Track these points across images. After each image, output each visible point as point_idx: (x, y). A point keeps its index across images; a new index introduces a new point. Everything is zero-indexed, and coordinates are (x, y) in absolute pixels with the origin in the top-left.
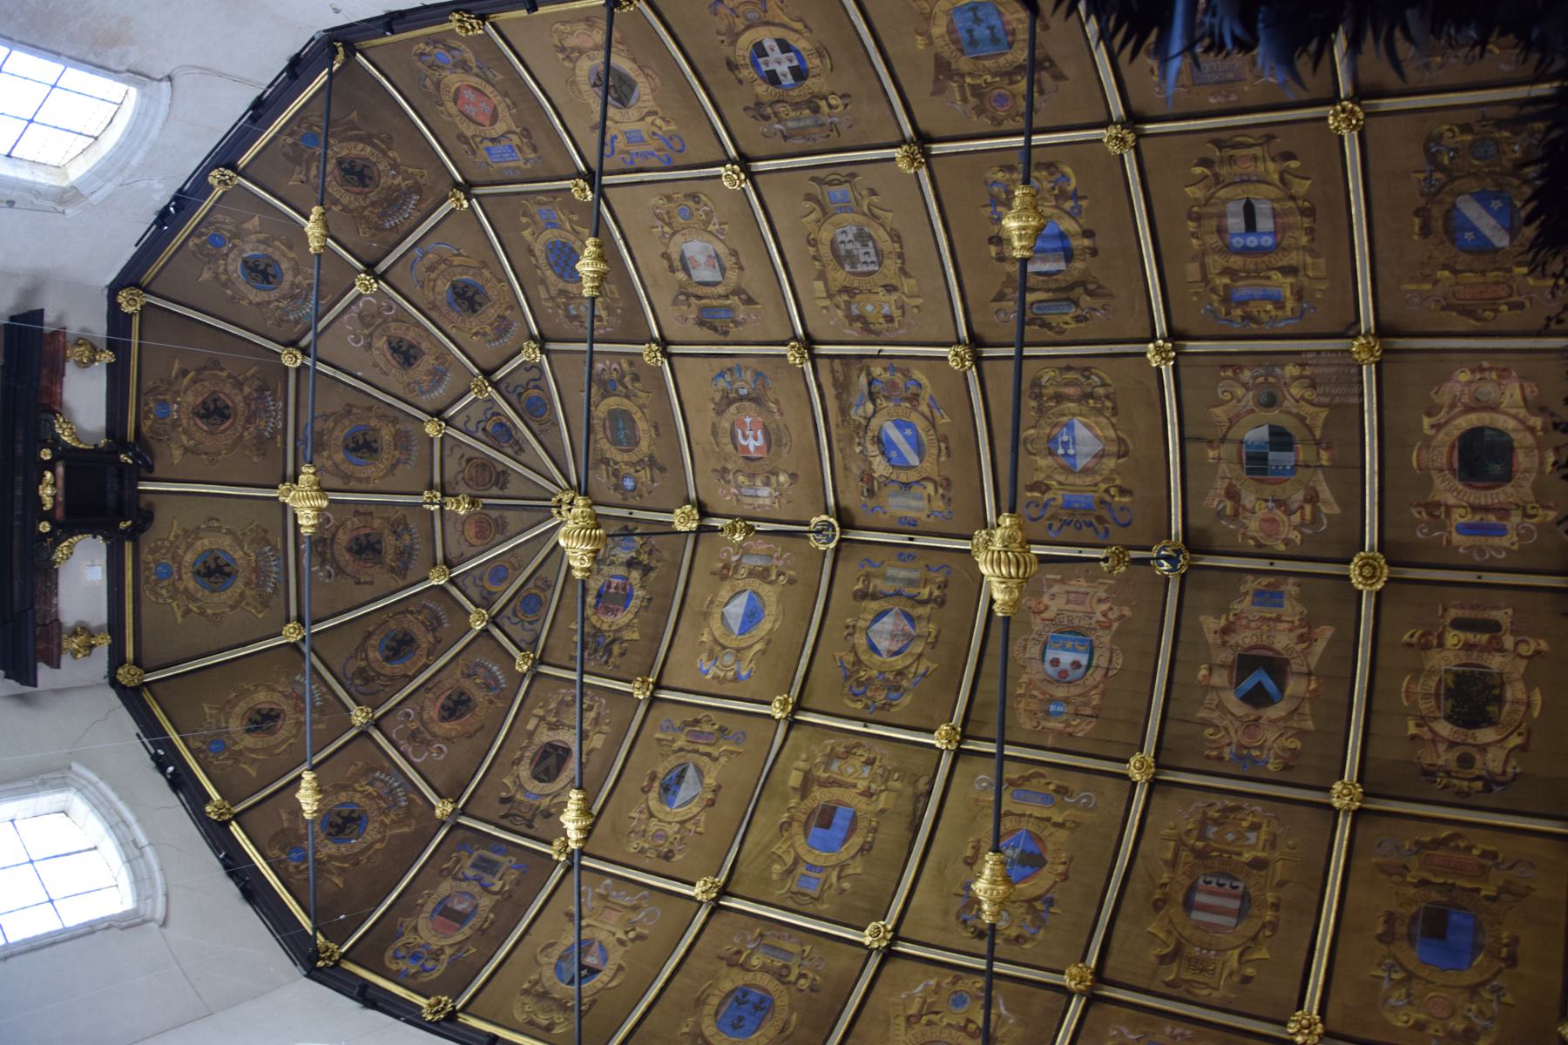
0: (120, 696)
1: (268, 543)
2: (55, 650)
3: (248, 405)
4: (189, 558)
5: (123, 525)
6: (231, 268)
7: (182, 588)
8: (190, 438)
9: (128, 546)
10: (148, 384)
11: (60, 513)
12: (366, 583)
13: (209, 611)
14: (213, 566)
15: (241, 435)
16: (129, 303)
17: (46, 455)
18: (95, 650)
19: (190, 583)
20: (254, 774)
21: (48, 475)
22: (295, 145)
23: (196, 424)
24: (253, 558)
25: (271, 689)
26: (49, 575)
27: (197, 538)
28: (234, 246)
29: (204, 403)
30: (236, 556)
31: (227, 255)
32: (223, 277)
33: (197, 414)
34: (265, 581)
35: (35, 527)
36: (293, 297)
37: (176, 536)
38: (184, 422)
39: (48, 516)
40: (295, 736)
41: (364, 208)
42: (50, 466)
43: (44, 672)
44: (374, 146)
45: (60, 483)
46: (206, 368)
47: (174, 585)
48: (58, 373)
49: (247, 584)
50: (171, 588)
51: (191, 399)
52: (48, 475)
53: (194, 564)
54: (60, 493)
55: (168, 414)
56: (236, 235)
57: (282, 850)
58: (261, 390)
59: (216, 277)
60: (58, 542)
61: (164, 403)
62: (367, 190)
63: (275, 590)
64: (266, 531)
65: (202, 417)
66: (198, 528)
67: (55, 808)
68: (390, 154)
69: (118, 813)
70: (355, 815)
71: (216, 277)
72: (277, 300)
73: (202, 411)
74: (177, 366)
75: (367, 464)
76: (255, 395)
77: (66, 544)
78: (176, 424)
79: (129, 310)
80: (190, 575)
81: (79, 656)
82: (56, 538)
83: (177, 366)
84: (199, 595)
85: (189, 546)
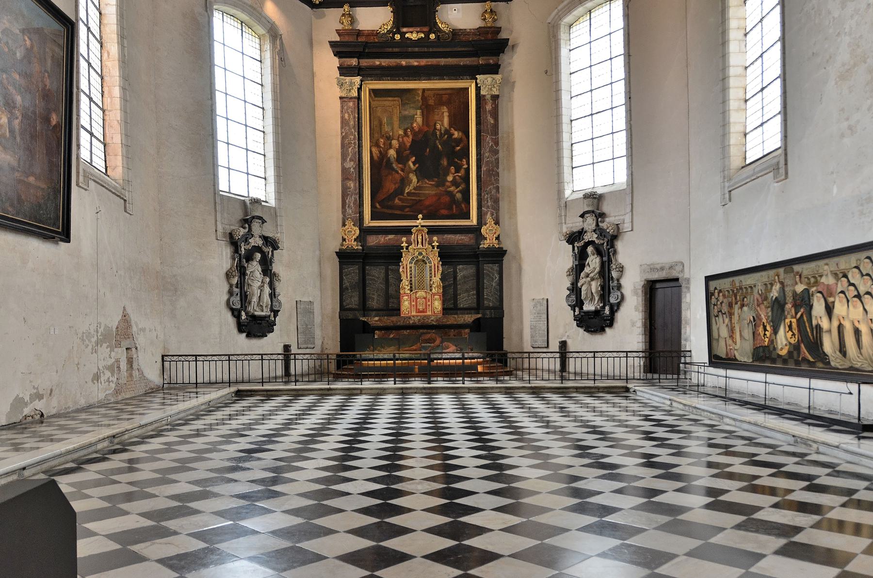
2: (493, 29)
11: (426, 29)
17: (397, 37)
18: (494, 9)
21: (407, 35)
26: (456, 33)
35: (433, 42)
42: (403, 34)
43: (503, 35)
45: (411, 29)
48: (359, 33)
52: (407, 35)
54: (415, 30)
60: (440, 30)
77: (440, 25)
81: (496, 17)
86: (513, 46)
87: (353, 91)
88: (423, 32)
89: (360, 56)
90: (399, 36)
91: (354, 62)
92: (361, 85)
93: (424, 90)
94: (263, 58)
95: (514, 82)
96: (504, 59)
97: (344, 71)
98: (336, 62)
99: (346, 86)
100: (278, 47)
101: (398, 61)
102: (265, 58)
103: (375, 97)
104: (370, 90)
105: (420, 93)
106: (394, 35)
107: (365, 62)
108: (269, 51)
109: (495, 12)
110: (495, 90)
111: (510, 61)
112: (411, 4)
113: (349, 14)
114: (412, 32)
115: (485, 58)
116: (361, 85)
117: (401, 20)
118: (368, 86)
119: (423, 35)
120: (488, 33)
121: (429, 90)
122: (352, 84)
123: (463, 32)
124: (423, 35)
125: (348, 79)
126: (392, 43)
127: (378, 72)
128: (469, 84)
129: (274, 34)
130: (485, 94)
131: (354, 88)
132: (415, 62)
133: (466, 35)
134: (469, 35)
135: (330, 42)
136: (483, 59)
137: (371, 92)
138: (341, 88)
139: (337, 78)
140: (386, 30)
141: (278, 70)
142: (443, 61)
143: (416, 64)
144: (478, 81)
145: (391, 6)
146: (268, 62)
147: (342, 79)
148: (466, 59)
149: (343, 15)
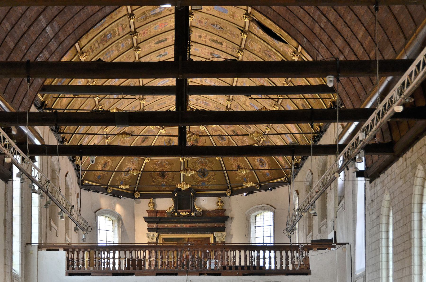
0: (233, 195)
3: (160, 167)
4: (200, 179)
5: (192, 195)
6: (127, 178)
7: (207, 180)
8: (170, 179)
9: (197, 192)
10: (157, 189)
11: (189, 211)
12: (205, 141)
13: (213, 174)
14: (202, 173)
15: (168, 168)
17: (176, 214)
19: (206, 179)
20: (251, 175)
21: (180, 213)
22: (100, 179)
23: (166, 178)
24: (200, 165)
25: (232, 164)
27: (195, 177)
28: (123, 179)
29: (161, 177)
30: (199, 169)
31: (125, 180)
32: (130, 178)
33: (164, 178)
34: (205, 162)
36: (133, 164)
37: (194, 182)
38: (166, 181)
39: (190, 213)
40: (243, 164)
41: (112, 161)
42: (178, 213)
44: (98, 165)
45: (182, 211)
46: (152, 176)
47: (206, 182)
48: (157, 212)
49: (206, 166)
50: (208, 183)
51: (160, 179)
52: (180, 213)
53: (201, 178)
56: (120, 180)
57: (267, 177)
58: (156, 165)
59: (130, 179)
60: (196, 211)
61: (162, 185)
62: (108, 162)
63: (207, 160)
64: (193, 162)
65: (164, 177)
66: (192, 177)
67: (254, 218)
68: (100, 162)
69: (255, 208)
70: (260, 160)
71: (130, 179)
72: (134, 166)
73: (163, 177)
74: (152, 183)
75: (174, 141)
76: (158, 166)
77: (196, 208)
78: (166, 182)
79: (139, 195)
80: (204, 178)
81: (223, 205)
82: (195, 211)
83: (152, 183)
84: (209, 176)
85: (197, 179)
86: (232, 218)
87: (154, 239)
89: (157, 223)
90: (177, 214)
91: (155, 225)
92: (158, 237)
93: (189, 238)
94: (114, 230)
95: (232, 235)
96: (227, 224)
97: (150, 230)
98: (146, 225)
99: (151, 237)
100: (121, 224)
101: (176, 225)
102: (115, 230)
103: (165, 241)
104: (162, 238)
105: (187, 240)
106: (174, 213)
107: (160, 225)
108: (117, 227)
109: (223, 202)
110: (223, 239)
111: (230, 224)
112: (183, 197)
113: (153, 202)
114: (183, 212)
115: (218, 224)
116: (158, 237)
118: (162, 236)
119: (188, 214)
120: (220, 212)
121: (191, 238)
122: (153, 236)
123: (207, 211)
124: (188, 214)
125: (152, 234)
127: (166, 230)
128: (210, 236)
129: (119, 219)
130: (218, 241)
131: (155, 238)
132: (184, 225)
133: (209, 212)
134: (211, 212)
135: (144, 217)
136: (217, 225)
137: (163, 239)
138: (148, 238)
139: (147, 234)
140: (170, 211)
141: (121, 235)
142: (198, 225)
143: (185, 226)
144: (215, 235)
146: (116, 232)
147: (149, 234)
148: (209, 224)
149: (150, 203)
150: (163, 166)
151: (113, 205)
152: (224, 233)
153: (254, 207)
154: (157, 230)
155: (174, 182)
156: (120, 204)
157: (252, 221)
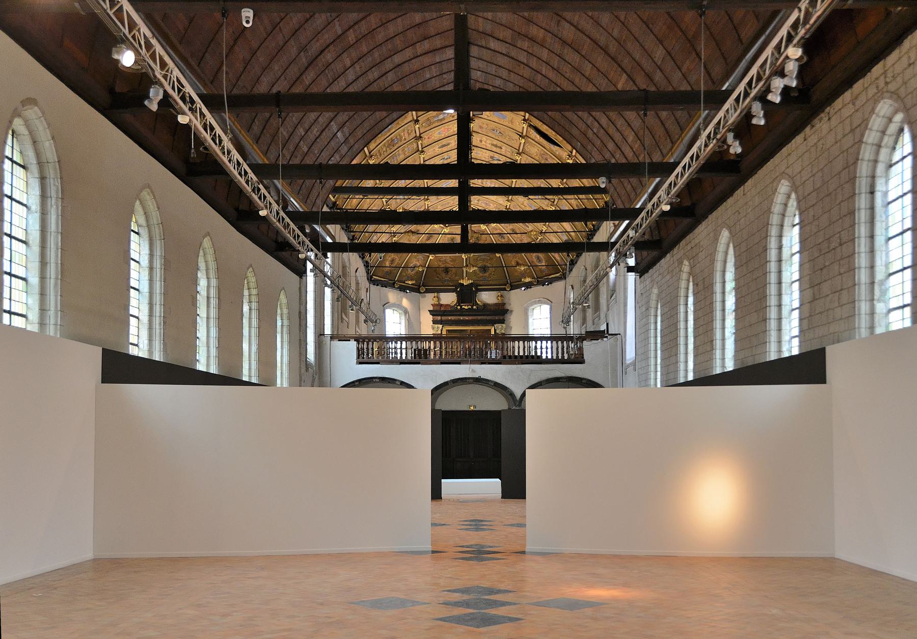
1: (477, 259)
4: (481, 275)
5: (474, 289)
9: (479, 287)
11: (472, 304)
16: (423, 289)
17: (459, 307)
19: (487, 274)
25: (511, 261)
26: (485, 305)
35: (475, 310)
39: (472, 306)
42: (461, 306)
48: (441, 305)
51: (444, 275)
55: (448, 279)
58: (440, 261)
61: (445, 281)
79: (425, 290)
88: (471, 306)
89: (441, 316)
91: (439, 318)
93: (471, 330)
95: (512, 327)
96: (507, 316)
97: (435, 322)
99: (436, 329)
101: (459, 317)
105: (469, 331)
107: (444, 318)
114: (465, 306)
117: (461, 299)
121: (473, 330)
125: (436, 326)
126: (456, 310)
129: (406, 312)
142: (479, 318)
143: (467, 319)
145: (456, 293)
149: (434, 297)
150: (446, 262)
151: (400, 299)
152: (504, 325)
153: (532, 301)
154: (441, 322)
155: (457, 278)
156: (407, 298)
157: (530, 314)
